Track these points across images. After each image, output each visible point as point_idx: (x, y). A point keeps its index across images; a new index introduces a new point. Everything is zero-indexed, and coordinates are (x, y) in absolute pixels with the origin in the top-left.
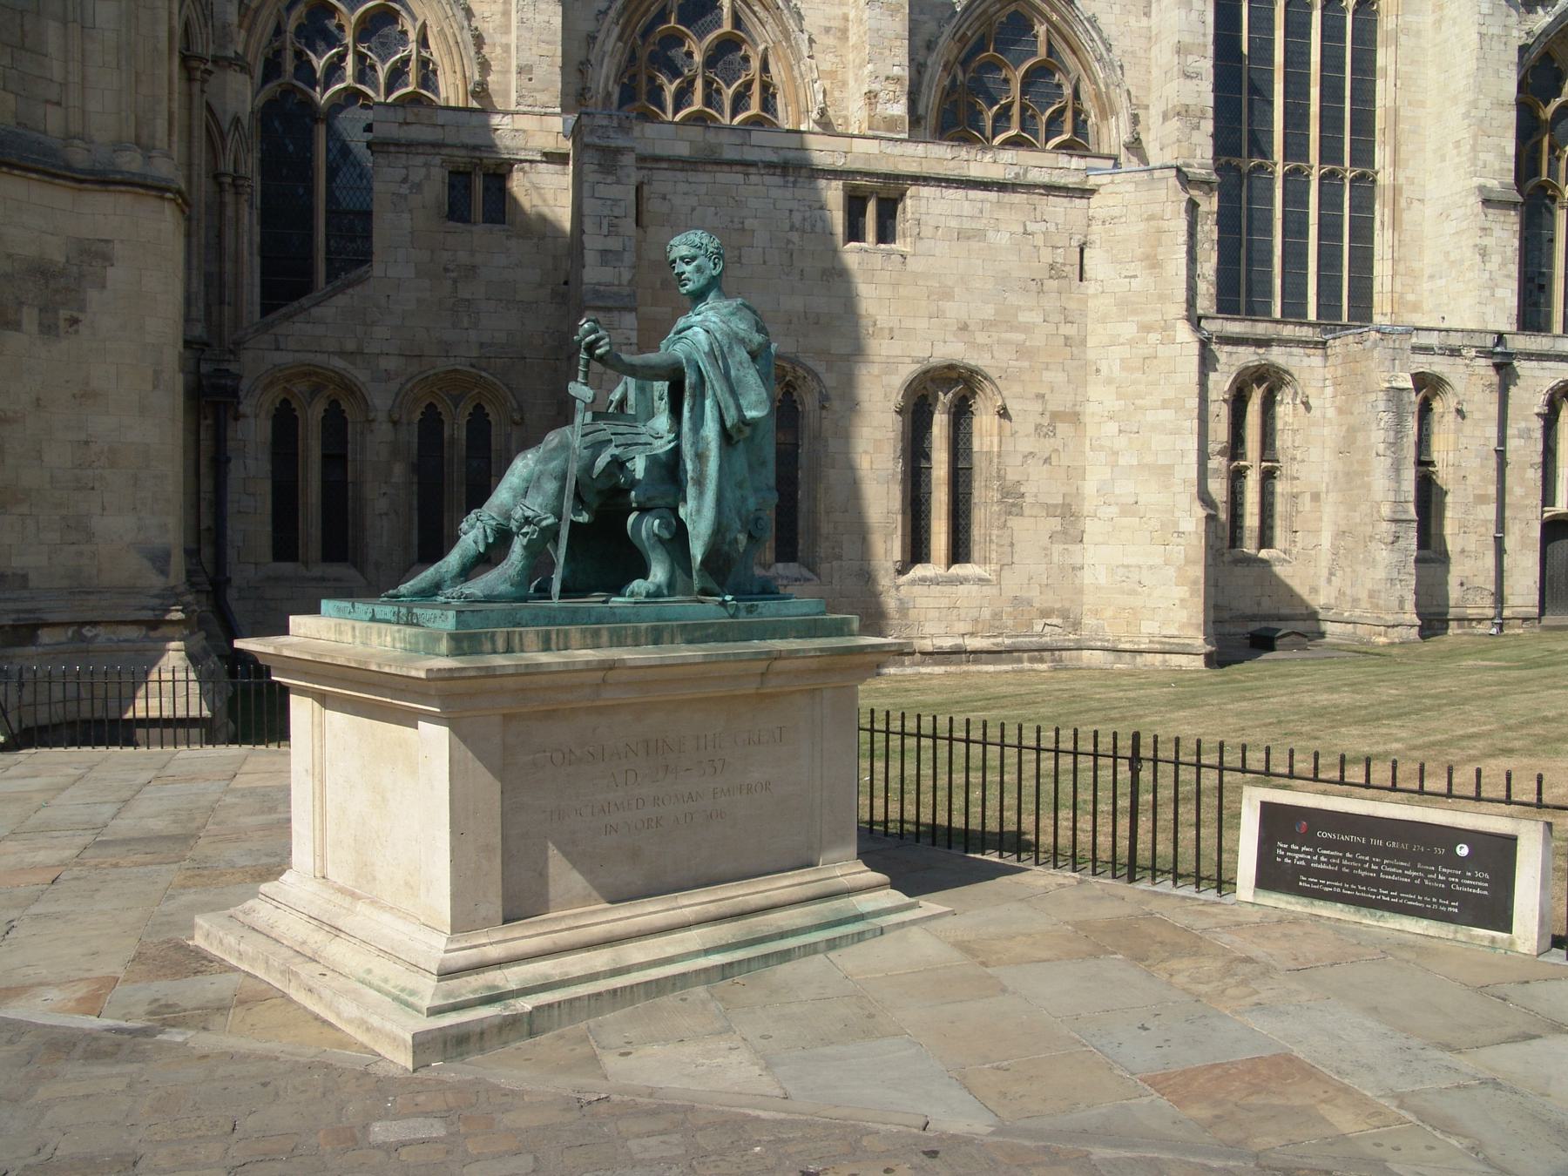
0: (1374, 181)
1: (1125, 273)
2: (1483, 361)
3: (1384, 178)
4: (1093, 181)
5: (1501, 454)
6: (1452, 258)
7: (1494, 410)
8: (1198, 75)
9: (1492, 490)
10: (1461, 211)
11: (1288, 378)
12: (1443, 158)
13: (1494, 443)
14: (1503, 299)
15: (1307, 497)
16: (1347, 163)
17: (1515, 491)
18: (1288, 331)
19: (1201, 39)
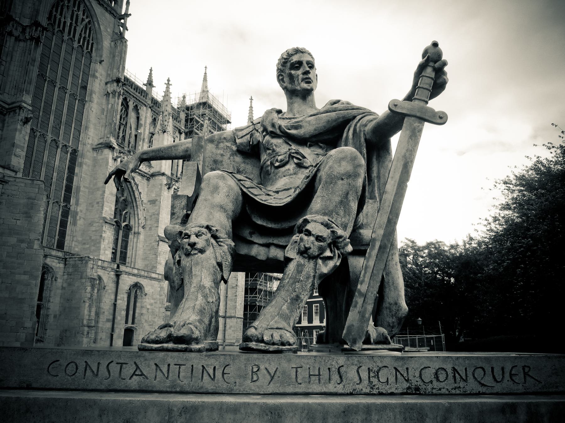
0: (69, 209)
1: (14, 218)
2: (113, 273)
3: (72, 208)
4: (6, 178)
5: (115, 305)
6: (93, 238)
7: (114, 289)
8: (19, 156)
9: (111, 317)
10: (97, 224)
11: (51, 270)
12: (93, 206)
13: (113, 301)
14: (107, 255)
15: (53, 316)
16: (62, 201)
17: (118, 318)
18: (54, 253)
19: (22, 145)
